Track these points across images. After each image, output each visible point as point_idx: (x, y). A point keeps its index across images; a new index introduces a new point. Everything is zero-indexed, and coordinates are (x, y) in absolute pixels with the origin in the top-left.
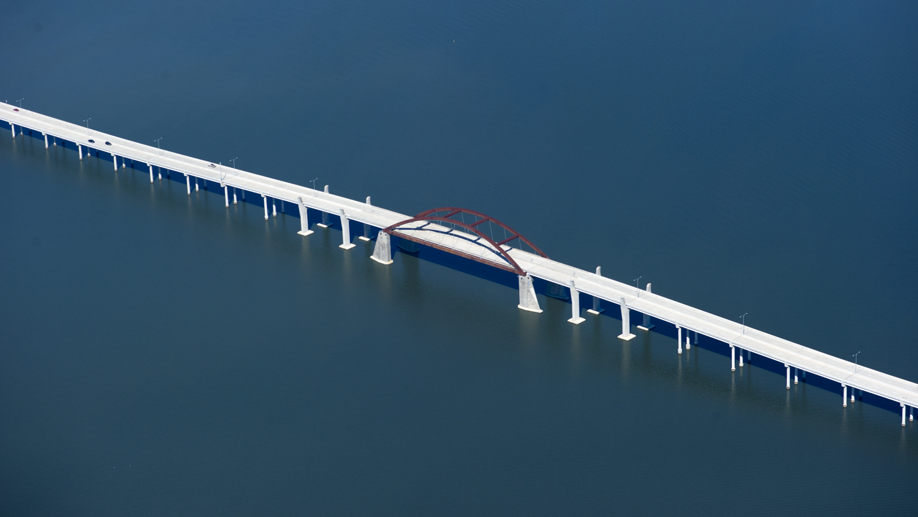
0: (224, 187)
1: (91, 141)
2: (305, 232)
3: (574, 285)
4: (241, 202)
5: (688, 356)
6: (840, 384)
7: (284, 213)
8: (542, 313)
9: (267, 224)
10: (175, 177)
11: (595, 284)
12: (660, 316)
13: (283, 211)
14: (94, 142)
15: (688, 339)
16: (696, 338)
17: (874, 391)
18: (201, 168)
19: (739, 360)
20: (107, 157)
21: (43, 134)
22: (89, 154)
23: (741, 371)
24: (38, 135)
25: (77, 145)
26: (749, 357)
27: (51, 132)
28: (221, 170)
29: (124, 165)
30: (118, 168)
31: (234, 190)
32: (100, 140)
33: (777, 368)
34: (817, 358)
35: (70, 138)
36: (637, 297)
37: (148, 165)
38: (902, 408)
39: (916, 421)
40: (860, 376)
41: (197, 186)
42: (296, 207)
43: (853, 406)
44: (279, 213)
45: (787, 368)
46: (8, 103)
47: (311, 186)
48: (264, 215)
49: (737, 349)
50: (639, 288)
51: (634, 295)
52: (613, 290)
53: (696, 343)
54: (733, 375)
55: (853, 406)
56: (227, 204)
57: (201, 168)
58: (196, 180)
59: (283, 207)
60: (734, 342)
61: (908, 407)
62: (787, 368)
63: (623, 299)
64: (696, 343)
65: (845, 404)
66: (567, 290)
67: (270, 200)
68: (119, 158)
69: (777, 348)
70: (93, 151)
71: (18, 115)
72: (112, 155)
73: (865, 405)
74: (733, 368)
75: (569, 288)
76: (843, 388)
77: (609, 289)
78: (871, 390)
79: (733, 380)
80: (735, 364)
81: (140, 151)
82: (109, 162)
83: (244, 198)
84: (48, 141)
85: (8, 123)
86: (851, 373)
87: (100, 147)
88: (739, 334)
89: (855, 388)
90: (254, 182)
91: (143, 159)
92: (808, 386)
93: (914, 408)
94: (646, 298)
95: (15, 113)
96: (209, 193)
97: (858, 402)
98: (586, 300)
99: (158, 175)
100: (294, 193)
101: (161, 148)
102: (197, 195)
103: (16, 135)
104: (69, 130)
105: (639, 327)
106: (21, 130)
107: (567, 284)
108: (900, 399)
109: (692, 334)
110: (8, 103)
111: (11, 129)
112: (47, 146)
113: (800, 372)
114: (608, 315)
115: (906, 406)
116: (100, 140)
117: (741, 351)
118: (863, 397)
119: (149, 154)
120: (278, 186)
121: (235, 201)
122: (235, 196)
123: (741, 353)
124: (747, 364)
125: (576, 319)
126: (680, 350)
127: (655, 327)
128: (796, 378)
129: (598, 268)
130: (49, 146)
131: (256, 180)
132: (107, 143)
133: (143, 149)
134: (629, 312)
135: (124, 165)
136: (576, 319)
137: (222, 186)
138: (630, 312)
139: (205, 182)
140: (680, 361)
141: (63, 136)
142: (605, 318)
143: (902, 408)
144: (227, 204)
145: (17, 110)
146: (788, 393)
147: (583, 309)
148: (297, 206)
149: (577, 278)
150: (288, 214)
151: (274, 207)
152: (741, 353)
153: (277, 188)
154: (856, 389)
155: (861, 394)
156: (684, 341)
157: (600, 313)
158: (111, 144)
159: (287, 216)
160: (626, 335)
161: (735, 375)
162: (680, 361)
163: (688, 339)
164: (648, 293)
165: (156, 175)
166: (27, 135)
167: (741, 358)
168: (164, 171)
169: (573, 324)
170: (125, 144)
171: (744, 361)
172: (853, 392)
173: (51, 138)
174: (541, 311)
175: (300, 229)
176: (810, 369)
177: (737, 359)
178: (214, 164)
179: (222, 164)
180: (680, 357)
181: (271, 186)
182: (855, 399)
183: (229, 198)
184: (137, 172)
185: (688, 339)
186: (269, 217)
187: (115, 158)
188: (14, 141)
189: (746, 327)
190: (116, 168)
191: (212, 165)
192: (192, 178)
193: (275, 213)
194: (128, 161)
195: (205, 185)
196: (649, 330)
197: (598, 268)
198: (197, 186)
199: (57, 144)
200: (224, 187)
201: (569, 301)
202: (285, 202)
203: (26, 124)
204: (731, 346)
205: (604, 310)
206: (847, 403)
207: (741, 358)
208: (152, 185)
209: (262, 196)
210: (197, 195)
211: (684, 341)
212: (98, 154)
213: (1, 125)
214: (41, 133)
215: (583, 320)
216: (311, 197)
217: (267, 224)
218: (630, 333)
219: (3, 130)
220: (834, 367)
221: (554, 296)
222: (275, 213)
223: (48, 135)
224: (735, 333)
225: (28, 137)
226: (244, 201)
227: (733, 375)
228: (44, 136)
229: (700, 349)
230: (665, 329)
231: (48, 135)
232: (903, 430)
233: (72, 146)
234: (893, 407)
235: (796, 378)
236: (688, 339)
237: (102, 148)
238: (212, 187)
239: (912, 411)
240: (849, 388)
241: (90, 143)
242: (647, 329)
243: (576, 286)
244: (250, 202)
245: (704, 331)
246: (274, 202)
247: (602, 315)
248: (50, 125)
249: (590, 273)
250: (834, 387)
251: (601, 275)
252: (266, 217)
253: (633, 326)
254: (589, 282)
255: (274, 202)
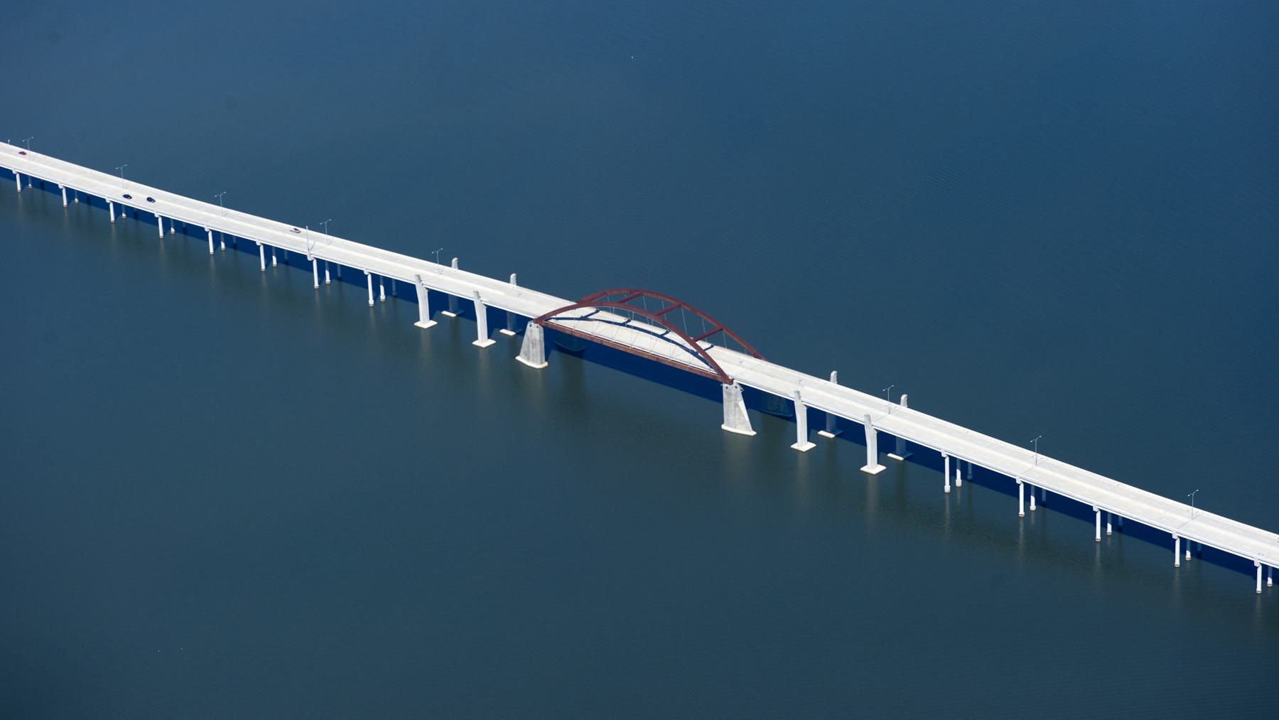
0: (312, 261)
1: (127, 196)
2: (425, 322)
3: (800, 398)
4: (336, 282)
5: (959, 496)
6: (1171, 535)
7: (396, 297)
8: (755, 436)
9: (372, 311)
10: (244, 246)
11: (830, 396)
12: (920, 439)
13: (394, 293)
14: (131, 198)
15: (959, 473)
16: (970, 471)
17: (1218, 544)
18: (280, 234)
19: (1106, 527)
20: (150, 218)
21: (60, 187)
22: (124, 215)
23: (1033, 516)
24: (52, 188)
25: (108, 201)
26: (1044, 497)
27: (71, 184)
28: (307, 236)
29: (173, 230)
30: (164, 233)
31: (327, 265)
32: (139, 195)
33: (1083, 512)
34: (1138, 498)
35: (97, 192)
36: (887, 414)
37: (206, 230)
38: (1257, 568)
39: (1277, 586)
40: (1198, 524)
41: (274, 259)
42: (412, 288)
43: (1188, 565)
44: (389, 297)
45: (1096, 513)
46: (11, 144)
47: (433, 259)
48: (369, 299)
49: (1028, 487)
50: (891, 401)
51: (885, 411)
52: (854, 404)
53: (970, 477)
54: (1021, 523)
55: (1188, 565)
56: (316, 285)
57: (280, 234)
58: (274, 251)
59: (394, 289)
60: (1023, 476)
61: (1265, 567)
62: (1096, 513)
63: (868, 416)
64: (970, 477)
65: (1177, 562)
66: (790, 404)
67: (376, 278)
68: (166, 221)
69: (1083, 484)
70: (129, 210)
71: (26, 161)
72: (156, 216)
73: (1205, 564)
74: (1022, 512)
75: (793, 402)
76: (1175, 540)
77: (849, 402)
78: (1214, 542)
79: (1021, 529)
80: (1024, 507)
81: (195, 211)
82: (472, 322)
83: (339, 275)
84: (67, 196)
85: (11, 171)
86: (1185, 520)
87: (139, 205)
88: (1030, 466)
89: (1192, 541)
90: (354, 253)
91: (199, 222)
92: (1125, 538)
93: (1273, 568)
94: (901, 414)
95: (21, 158)
96: (291, 268)
97: (1196, 560)
98: (817, 418)
99: (170, 229)
100: (410, 268)
101: (225, 206)
102: (275, 272)
103: (22, 188)
104: (97, 182)
105: (890, 455)
106: (30, 181)
107: (791, 395)
108: (1254, 555)
109: (964, 465)
110: (11, 143)
111: (16, 180)
112: (65, 203)
113: (1115, 518)
114: (847, 439)
115: (1263, 565)
116: (139, 195)
117: (1032, 488)
118: (1203, 553)
119: (207, 214)
120: (387, 260)
121: (328, 280)
122: (327, 273)
123: (1033, 491)
124: (1041, 507)
125: (803, 444)
126: (947, 488)
127: (912, 456)
128: (1109, 526)
129: (833, 374)
130: (68, 203)
131: (358, 250)
132: (150, 200)
133: (199, 208)
134: (876, 435)
135: (173, 230)
136: (803, 444)
137: (309, 259)
138: (877, 434)
139: (286, 254)
140: (947, 503)
141: (88, 189)
142: (843, 442)
143: (1257, 568)
144: (316, 285)
145: (23, 153)
146: (1098, 547)
147: (813, 431)
148: (414, 286)
149: (803, 387)
150: (400, 298)
151: (382, 288)
152: (1033, 491)
153: (387, 262)
154: (1192, 542)
155: (1199, 549)
156: (953, 475)
157: (836, 436)
158: (154, 201)
159: (400, 301)
160: (873, 467)
161: (1024, 522)
162: (947, 503)
163: (959, 473)
164: (903, 408)
165: (217, 244)
166: (83, 202)
167: (1033, 499)
168: (228, 238)
169: (797, 451)
170: (174, 201)
171: (1036, 503)
172: (1188, 545)
173: (71, 192)
174: (753, 433)
175: (418, 320)
176: (1052, 486)
177: (1027, 500)
178: (298, 228)
179: (309, 229)
180: (947, 498)
181: (378, 260)
182: (1273, 582)
183: (319, 276)
184: (191, 240)
185: (959, 473)
186: (374, 302)
187: (160, 220)
188: (20, 196)
189: (1040, 456)
190: (161, 234)
191: (296, 229)
192: (268, 248)
193: (383, 297)
194: (178, 224)
195: (286, 258)
196: (905, 459)
197: (833, 374)
198: (274, 259)
199: (80, 200)
200: (312, 261)
201: (793, 419)
202: (397, 281)
203: (35, 173)
204: (1018, 482)
205: (841, 432)
206: (1262, 588)
207: (1033, 499)
208: (212, 258)
209: (366, 273)
210: (275, 272)
211: (953, 475)
212: (136, 214)
213: (2, 174)
214: (57, 185)
215: (812, 445)
216: (433, 274)
217: (372, 311)
218: (878, 463)
219: (4, 181)
220: (1162, 512)
221: (772, 413)
222: (383, 297)
223: (67, 188)
224: (1024, 463)
225: (38, 191)
226: (340, 279)
227: (1021, 523)
228: (62, 190)
229: (974, 486)
230: (926, 458)
231: (66, 188)
232: (1259, 599)
233: (100, 203)
234: (1245, 566)
235: (1109, 526)
236: (959, 473)
237: (142, 206)
238: (295, 261)
239: (1270, 572)
240: (1183, 541)
241: (126, 200)
242: (901, 459)
243: (802, 399)
244: (347, 282)
245: (981, 461)
246: (381, 281)
247: (907, 462)
248: (70, 174)
249: (822, 380)
250: (1163, 539)
251: (838, 383)
252: (371, 302)
253: (882, 454)
254: (820, 392)
255: (381, 281)
